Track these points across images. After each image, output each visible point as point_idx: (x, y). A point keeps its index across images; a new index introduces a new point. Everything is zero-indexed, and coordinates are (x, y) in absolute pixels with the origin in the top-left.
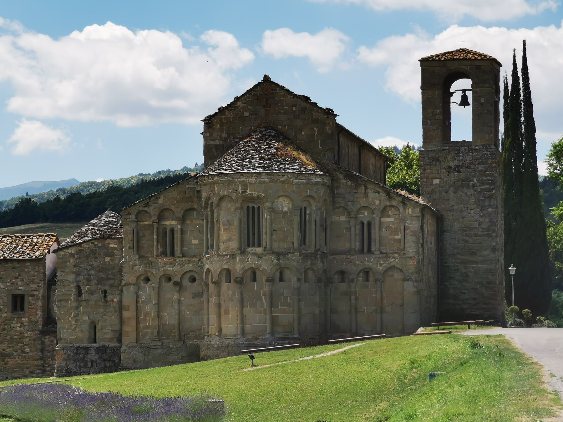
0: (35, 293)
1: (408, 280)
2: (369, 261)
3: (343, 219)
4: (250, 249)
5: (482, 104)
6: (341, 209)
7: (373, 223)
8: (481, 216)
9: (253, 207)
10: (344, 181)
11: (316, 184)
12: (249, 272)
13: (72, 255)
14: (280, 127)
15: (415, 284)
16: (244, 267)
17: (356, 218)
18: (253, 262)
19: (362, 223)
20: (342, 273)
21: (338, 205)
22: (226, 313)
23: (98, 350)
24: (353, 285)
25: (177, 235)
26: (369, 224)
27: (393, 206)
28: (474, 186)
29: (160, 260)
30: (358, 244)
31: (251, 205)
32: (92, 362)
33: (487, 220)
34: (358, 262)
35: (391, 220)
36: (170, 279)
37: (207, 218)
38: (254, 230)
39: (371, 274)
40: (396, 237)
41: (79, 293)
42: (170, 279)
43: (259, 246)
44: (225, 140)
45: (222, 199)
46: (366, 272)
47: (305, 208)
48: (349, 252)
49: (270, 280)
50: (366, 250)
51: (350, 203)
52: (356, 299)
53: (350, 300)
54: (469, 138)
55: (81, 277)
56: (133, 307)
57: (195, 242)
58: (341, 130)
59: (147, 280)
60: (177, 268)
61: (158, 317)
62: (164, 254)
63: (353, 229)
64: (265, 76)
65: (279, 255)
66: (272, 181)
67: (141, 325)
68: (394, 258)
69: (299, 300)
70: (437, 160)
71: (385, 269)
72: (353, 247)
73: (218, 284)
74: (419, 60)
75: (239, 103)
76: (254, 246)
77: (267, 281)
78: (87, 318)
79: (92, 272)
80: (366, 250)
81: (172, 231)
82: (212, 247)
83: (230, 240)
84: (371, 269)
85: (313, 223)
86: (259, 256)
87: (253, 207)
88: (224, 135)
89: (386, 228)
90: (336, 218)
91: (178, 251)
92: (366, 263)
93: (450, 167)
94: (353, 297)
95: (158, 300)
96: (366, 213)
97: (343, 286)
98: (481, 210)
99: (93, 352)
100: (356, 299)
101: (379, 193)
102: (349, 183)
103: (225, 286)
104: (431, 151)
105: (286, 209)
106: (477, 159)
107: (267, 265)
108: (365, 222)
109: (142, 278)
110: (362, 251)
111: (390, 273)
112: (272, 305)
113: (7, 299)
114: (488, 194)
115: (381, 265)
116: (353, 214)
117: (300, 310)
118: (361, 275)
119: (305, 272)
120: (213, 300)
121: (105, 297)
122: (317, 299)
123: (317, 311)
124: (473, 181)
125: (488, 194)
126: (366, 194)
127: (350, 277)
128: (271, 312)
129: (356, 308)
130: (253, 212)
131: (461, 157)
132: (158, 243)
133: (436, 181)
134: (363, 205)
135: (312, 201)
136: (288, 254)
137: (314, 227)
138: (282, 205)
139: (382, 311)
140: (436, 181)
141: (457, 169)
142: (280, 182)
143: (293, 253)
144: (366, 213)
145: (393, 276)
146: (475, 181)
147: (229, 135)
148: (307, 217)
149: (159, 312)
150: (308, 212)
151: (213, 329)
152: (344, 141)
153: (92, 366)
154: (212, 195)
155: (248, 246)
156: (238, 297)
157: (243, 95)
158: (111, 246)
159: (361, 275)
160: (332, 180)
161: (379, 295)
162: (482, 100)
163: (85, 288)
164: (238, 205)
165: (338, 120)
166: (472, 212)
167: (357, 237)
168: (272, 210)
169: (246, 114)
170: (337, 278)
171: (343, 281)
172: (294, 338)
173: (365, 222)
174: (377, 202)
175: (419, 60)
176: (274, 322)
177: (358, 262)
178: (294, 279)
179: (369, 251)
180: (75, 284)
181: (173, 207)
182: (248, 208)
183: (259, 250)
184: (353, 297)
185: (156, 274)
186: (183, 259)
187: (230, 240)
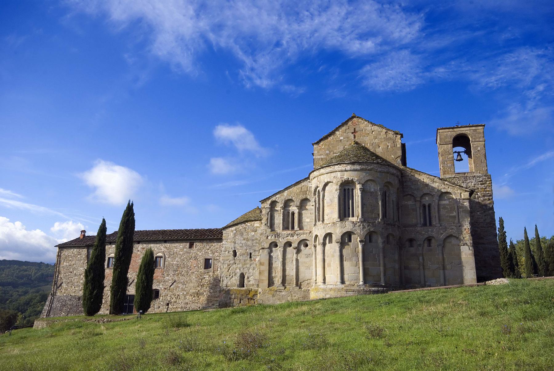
0: (218, 258)
2: (432, 231)
3: (410, 203)
5: (479, 151)
6: (409, 196)
7: (433, 204)
9: (349, 189)
11: (393, 174)
13: (232, 231)
16: (342, 231)
19: (424, 206)
20: (411, 241)
22: (329, 265)
24: (420, 248)
25: (296, 216)
26: (429, 206)
30: (422, 220)
31: (347, 188)
33: (489, 217)
36: (290, 246)
37: (315, 201)
39: (433, 241)
40: (451, 215)
42: (290, 246)
43: (353, 216)
44: (327, 155)
45: (326, 185)
46: (429, 240)
48: (415, 225)
50: (428, 224)
52: (423, 259)
53: (419, 260)
57: (308, 220)
59: (276, 246)
60: (295, 237)
63: (418, 209)
71: (444, 237)
72: (419, 222)
73: (324, 244)
80: (428, 224)
81: (293, 214)
82: (319, 220)
83: (332, 213)
84: (433, 237)
85: (392, 202)
87: (349, 189)
88: (328, 152)
89: (442, 208)
91: (296, 227)
92: (430, 233)
94: (421, 258)
96: (427, 198)
97: (412, 250)
98: (485, 212)
100: (423, 259)
103: (328, 246)
105: (372, 190)
108: (427, 205)
109: (273, 244)
110: (425, 225)
111: (448, 240)
113: (202, 263)
116: (418, 199)
118: (426, 242)
119: (388, 236)
120: (320, 257)
121: (251, 257)
122: (396, 257)
123: (397, 266)
127: (418, 243)
129: (423, 266)
130: (348, 193)
135: (390, 187)
137: (392, 206)
138: (370, 187)
139: (444, 268)
144: (427, 198)
145: (450, 242)
147: (330, 152)
148: (387, 198)
150: (387, 195)
151: (320, 279)
154: (318, 183)
156: (338, 253)
158: (255, 225)
161: (440, 256)
162: (479, 149)
164: (338, 187)
167: (422, 215)
170: (407, 244)
171: (411, 246)
173: (427, 205)
177: (423, 232)
178: (380, 241)
179: (430, 224)
180: (233, 249)
184: (421, 258)
185: (281, 242)
186: (300, 232)
187: (332, 213)
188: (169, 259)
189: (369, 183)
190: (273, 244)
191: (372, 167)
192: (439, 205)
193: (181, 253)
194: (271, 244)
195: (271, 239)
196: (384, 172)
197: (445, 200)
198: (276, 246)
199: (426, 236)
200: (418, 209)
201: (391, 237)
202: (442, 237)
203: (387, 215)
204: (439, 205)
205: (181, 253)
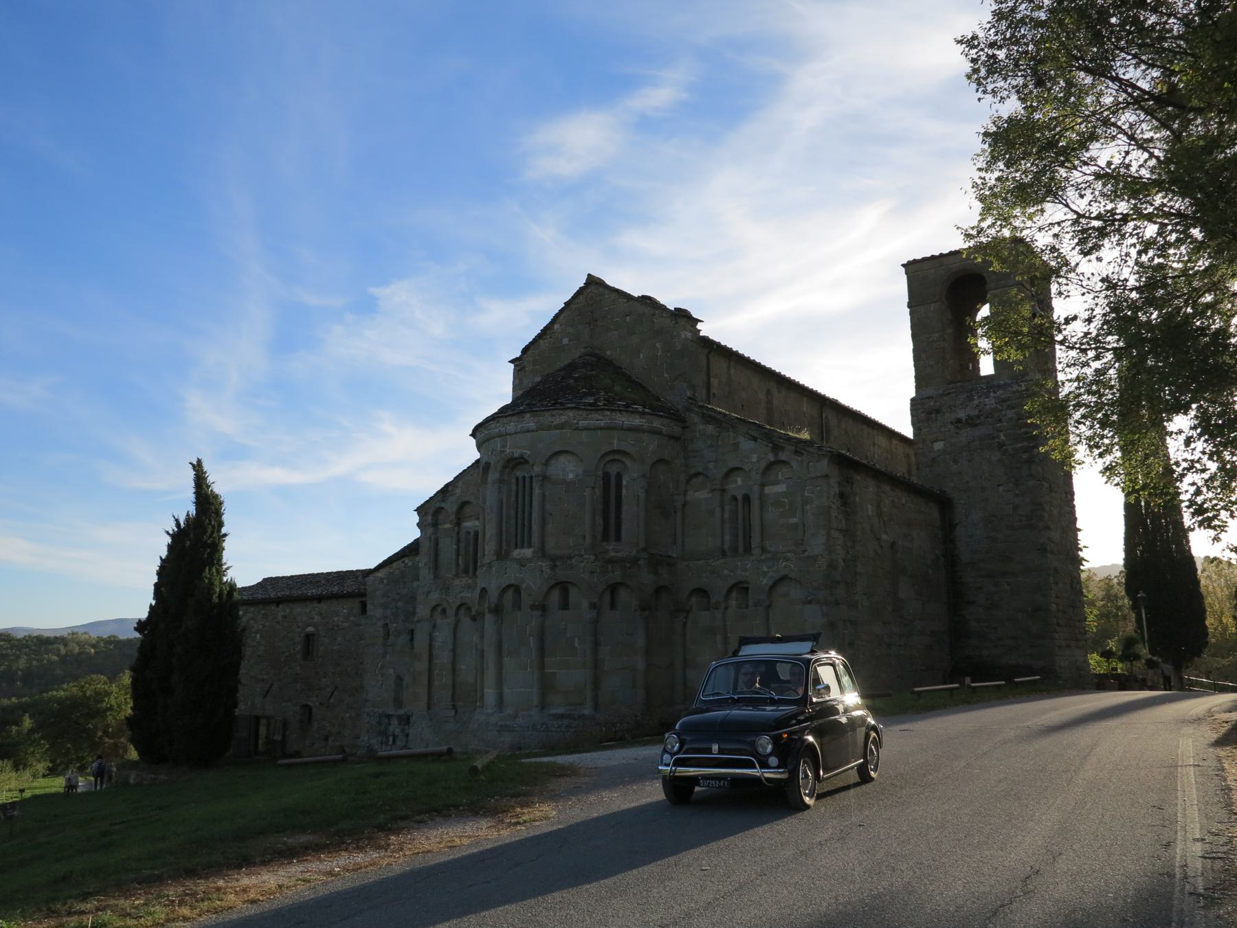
1: (810, 602)
3: (703, 495)
4: (516, 553)
6: (701, 478)
8: (1017, 495)
10: (701, 427)
11: (632, 429)
12: (510, 593)
13: (382, 580)
14: (609, 353)
15: (824, 608)
17: (723, 491)
18: (512, 574)
19: (735, 498)
20: (702, 592)
21: (693, 472)
23: (400, 718)
26: (747, 499)
27: (783, 462)
28: (1001, 445)
29: (457, 582)
30: (727, 538)
31: (519, 473)
32: (395, 737)
34: (726, 572)
35: (781, 488)
38: (523, 519)
41: (387, 635)
43: (530, 546)
46: (742, 588)
47: (619, 476)
49: (543, 608)
50: (741, 549)
51: (711, 465)
54: (992, 372)
55: (389, 612)
56: (426, 656)
58: (709, 345)
61: (454, 670)
62: (466, 571)
64: (589, 275)
65: (554, 559)
66: (541, 428)
67: (436, 683)
68: (787, 560)
69: (596, 644)
70: (938, 411)
71: (770, 583)
74: (903, 265)
75: (556, 326)
76: (522, 547)
77: (533, 607)
78: (391, 671)
79: (400, 604)
80: (741, 549)
86: (522, 562)
90: (692, 495)
93: (959, 421)
95: (454, 644)
96: (739, 480)
99: (395, 722)
101: (755, 439)
102: (710, 429)
104: (929, 398)
105: (571, 476)
106: (1004, 401)
107: (534, 580)
108: (740, 497)
112: (542, 652)
114: (1025, 456)
115: (765, 574)
117: (597, 664)
123: (640, 664)
124: (999, 437)
125: (1025, 456)
126: (736, 446)
128: (542, 666)
131: (976, 402)
132: (458, 555)
133: (939, 446)
134: (731, 466)
135: (628, 462)
136: (570, 558)
140: (939, 446)
141: (971, 422)
142: (556, 427)
143: (581, 556)
144: (739, 480)
146: (1003, 437)
149: (454, 663)
150: (624, 482)
151: (490, 694)
152: (719, 365)
153: (394, 742)
155: (516, 547)
157: (561, 311)
159: (734, 594)
160: (683, 428)
163: (393, 627)
165: (705, 329)
166: (1001, 489)
168: (545, 478)
169: (565, 341)
172: (582, 717)
173: (740, 497)
174: (754, 458)
175: (903, 265)
176: (546, 686)
177: (726, 572)
179: (748, 549)
181: (472, 499)
182: (517, 479)
183: (528, 552)
184: (719, 638)
188: (326, 640)
189: (562, 459)
190: (439, 609)
191: (563, 419)
192: (762, 494)
193: (346, 625)
194: (434, 608)
195: (435, 597)
196: (600, 428)
197: (776, 483)
198: (444, 611)
199: (731, 582)
200: (718, 510)
201: (623, 594)
202: (765, 582)
203: (624, 533)
204: (762, 494)
205: (346, 625)
